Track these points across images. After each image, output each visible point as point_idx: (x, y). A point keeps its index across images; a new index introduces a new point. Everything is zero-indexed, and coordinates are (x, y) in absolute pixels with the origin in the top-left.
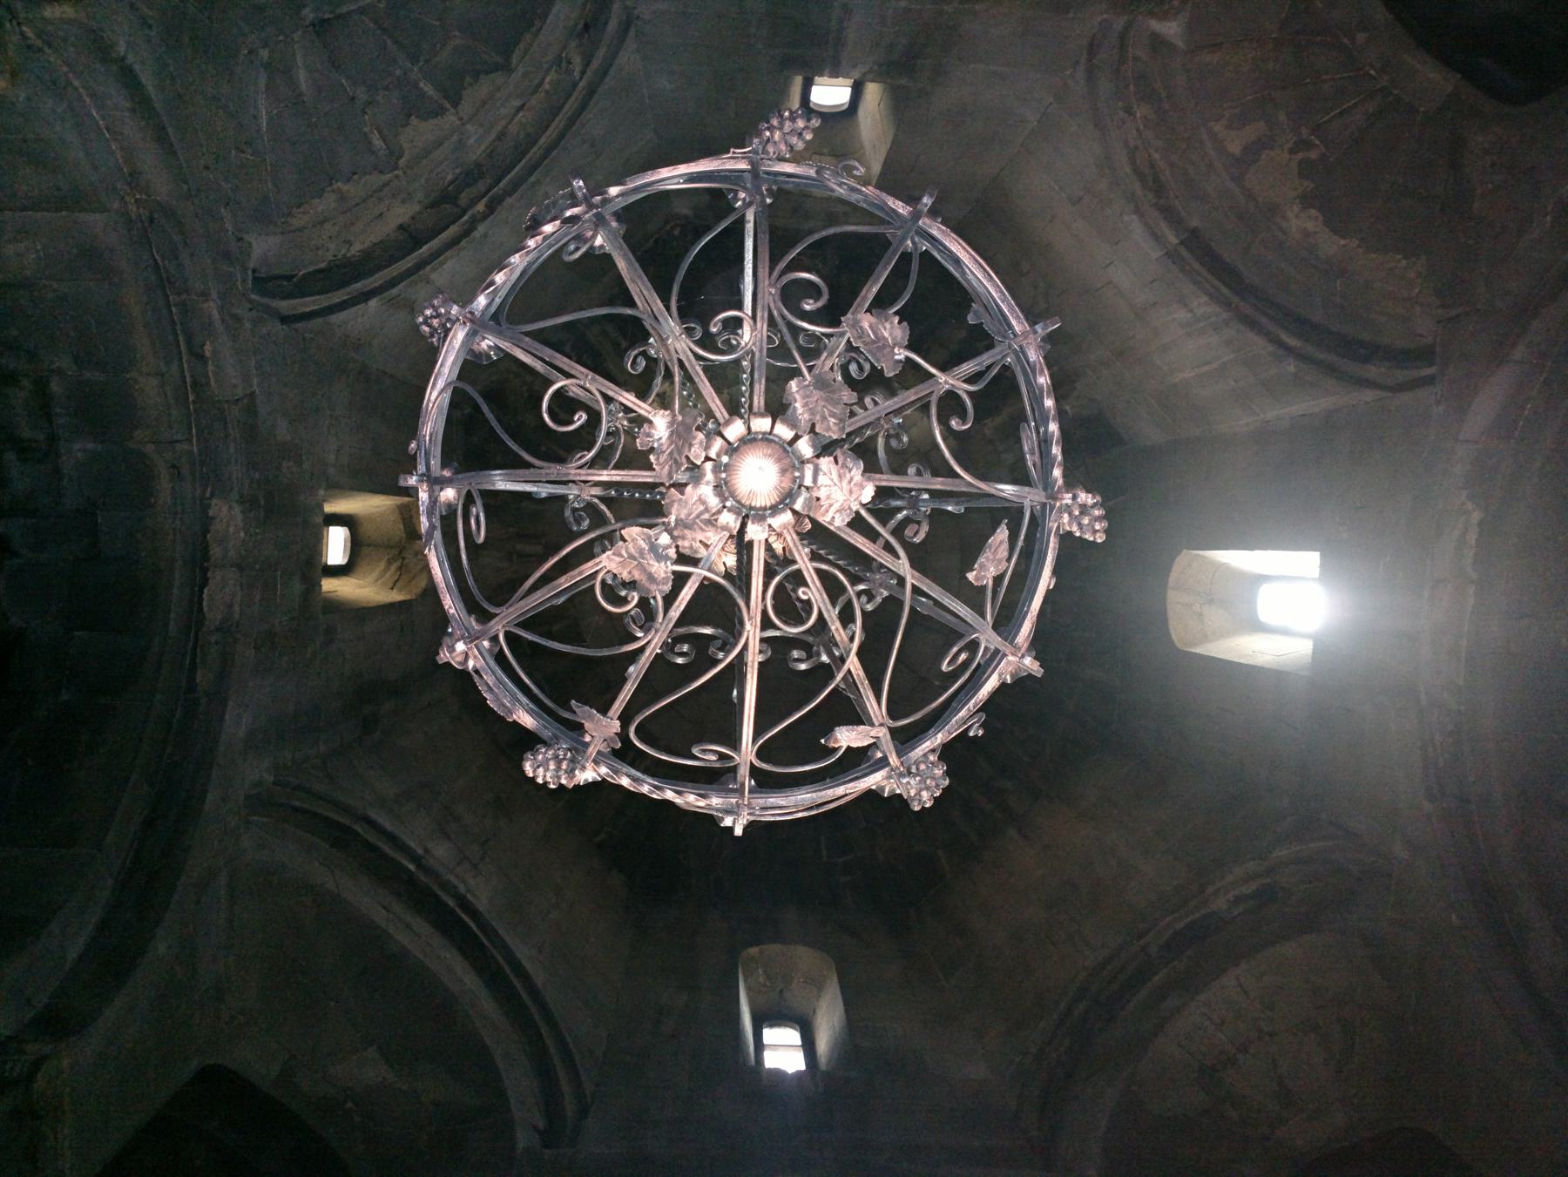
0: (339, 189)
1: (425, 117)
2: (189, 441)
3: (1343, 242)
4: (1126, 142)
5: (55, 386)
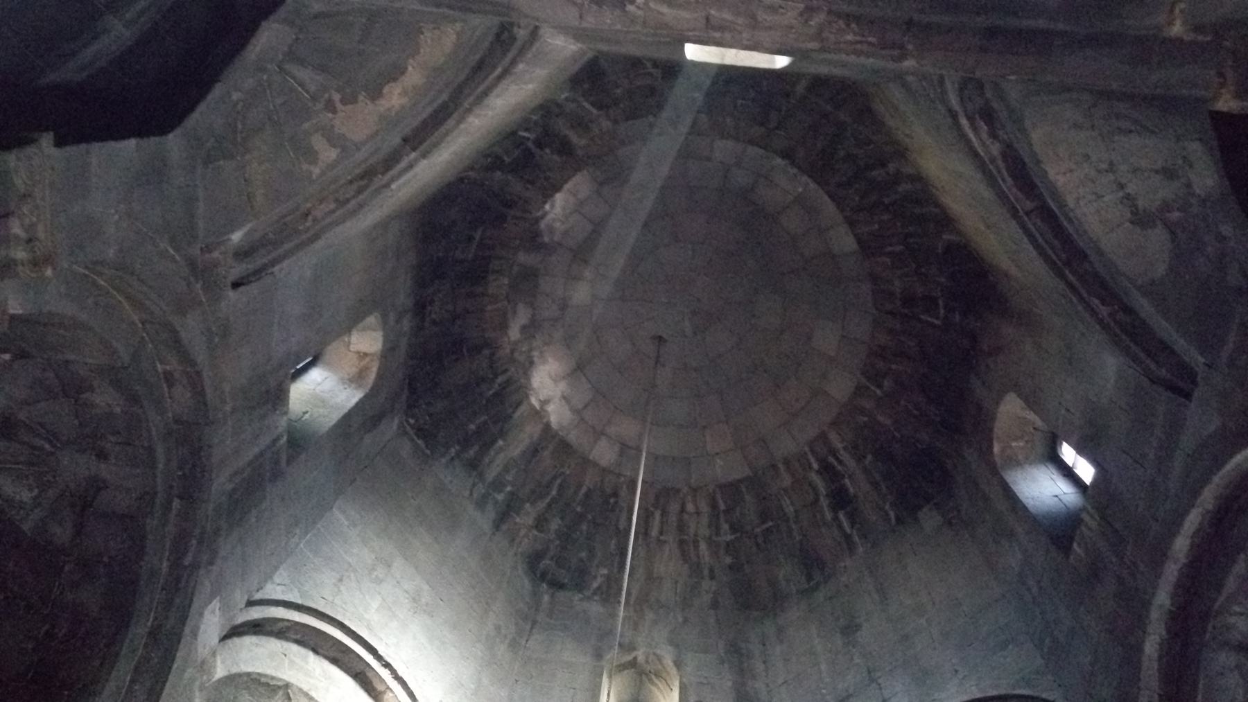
3: (410, 68)
4: (333, 211)
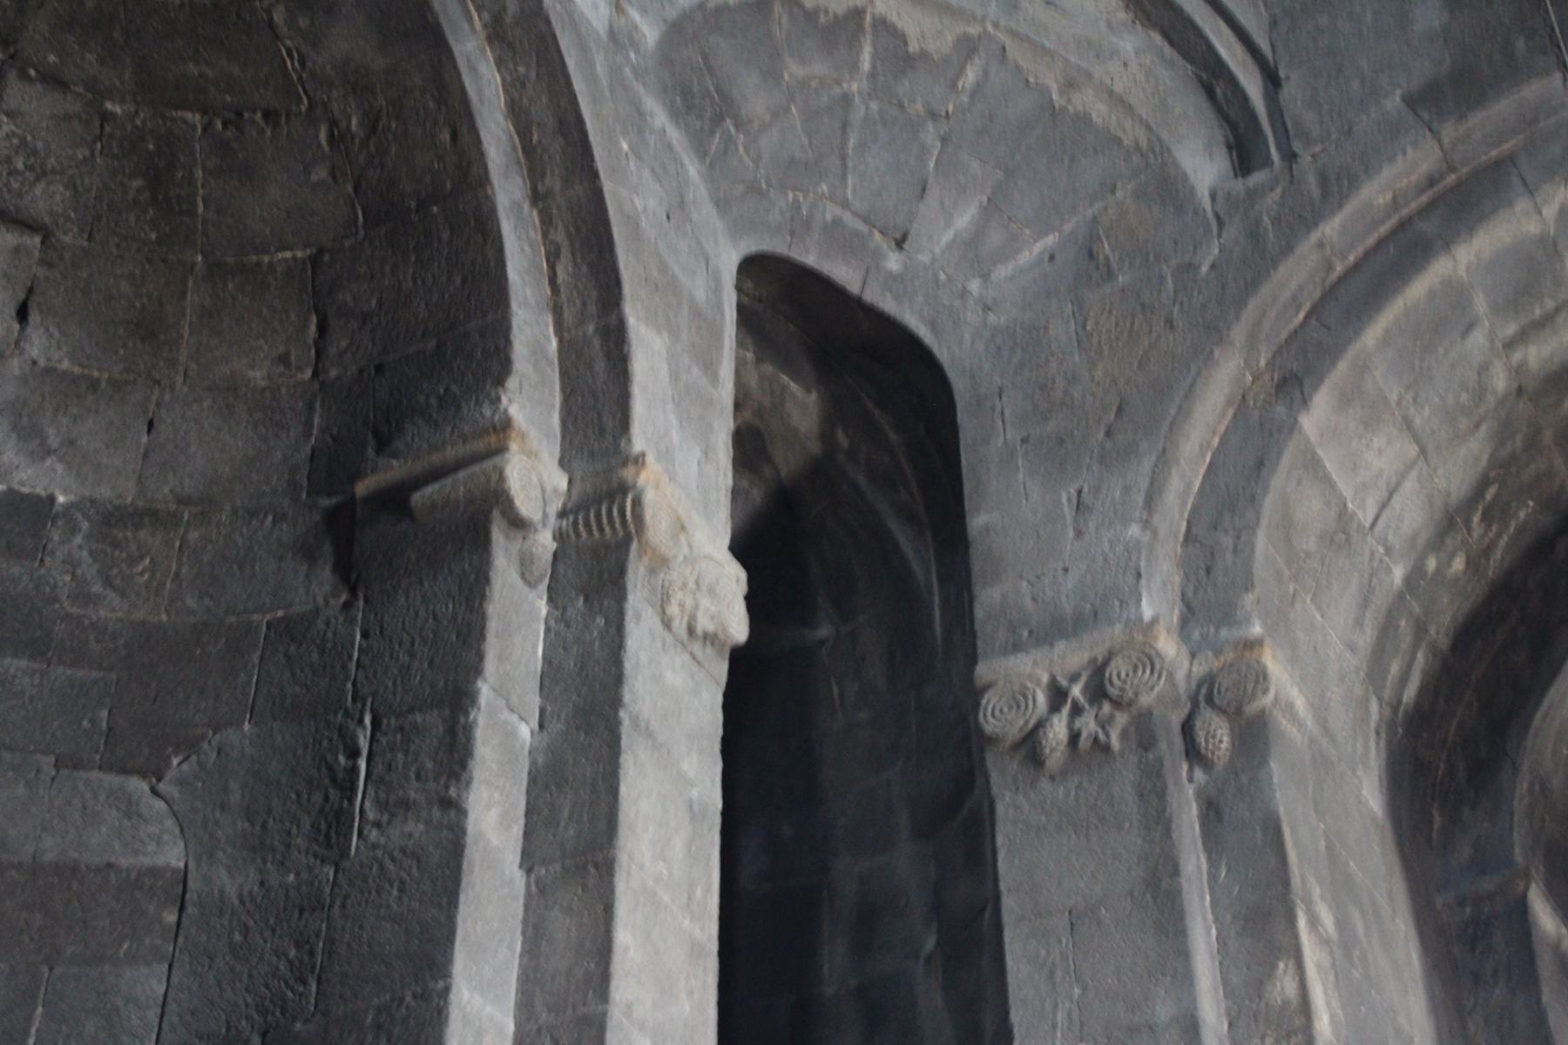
0: (1061, 93)
1: (902, 39)
2: (1511, 159)
5: (1511, 329)
